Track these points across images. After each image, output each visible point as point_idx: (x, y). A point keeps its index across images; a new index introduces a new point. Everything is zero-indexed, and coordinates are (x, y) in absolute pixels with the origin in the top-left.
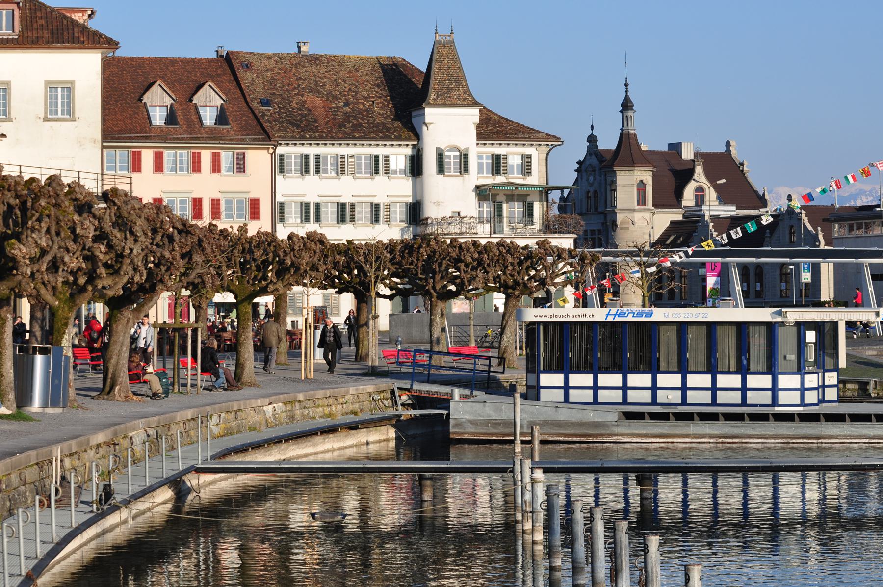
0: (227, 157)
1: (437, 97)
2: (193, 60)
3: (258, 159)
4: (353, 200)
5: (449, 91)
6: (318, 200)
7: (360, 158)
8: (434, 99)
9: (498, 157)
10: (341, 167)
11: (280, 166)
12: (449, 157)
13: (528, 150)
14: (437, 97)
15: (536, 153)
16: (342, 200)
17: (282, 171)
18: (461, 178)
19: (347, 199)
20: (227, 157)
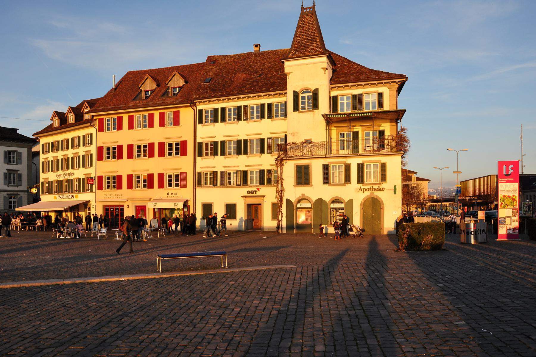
0: (169, 114)
1: (295, 53)
2: (184, 66)
3: (187, 114)
4: (246, 138)
5: (306, 47)
6: (223, 139)
7: (252, 108)
8: (293, 55)
9: (354, 97)
10: (240, 114)
11: (200, 118)
12: (303, 98)
13: (380, 89)
14: (295, 53)
15: (387, 91)
16: (239, 138)
17: (201, 122)
18: (312, 113)
19: (242, 137)
20: (169, 114)
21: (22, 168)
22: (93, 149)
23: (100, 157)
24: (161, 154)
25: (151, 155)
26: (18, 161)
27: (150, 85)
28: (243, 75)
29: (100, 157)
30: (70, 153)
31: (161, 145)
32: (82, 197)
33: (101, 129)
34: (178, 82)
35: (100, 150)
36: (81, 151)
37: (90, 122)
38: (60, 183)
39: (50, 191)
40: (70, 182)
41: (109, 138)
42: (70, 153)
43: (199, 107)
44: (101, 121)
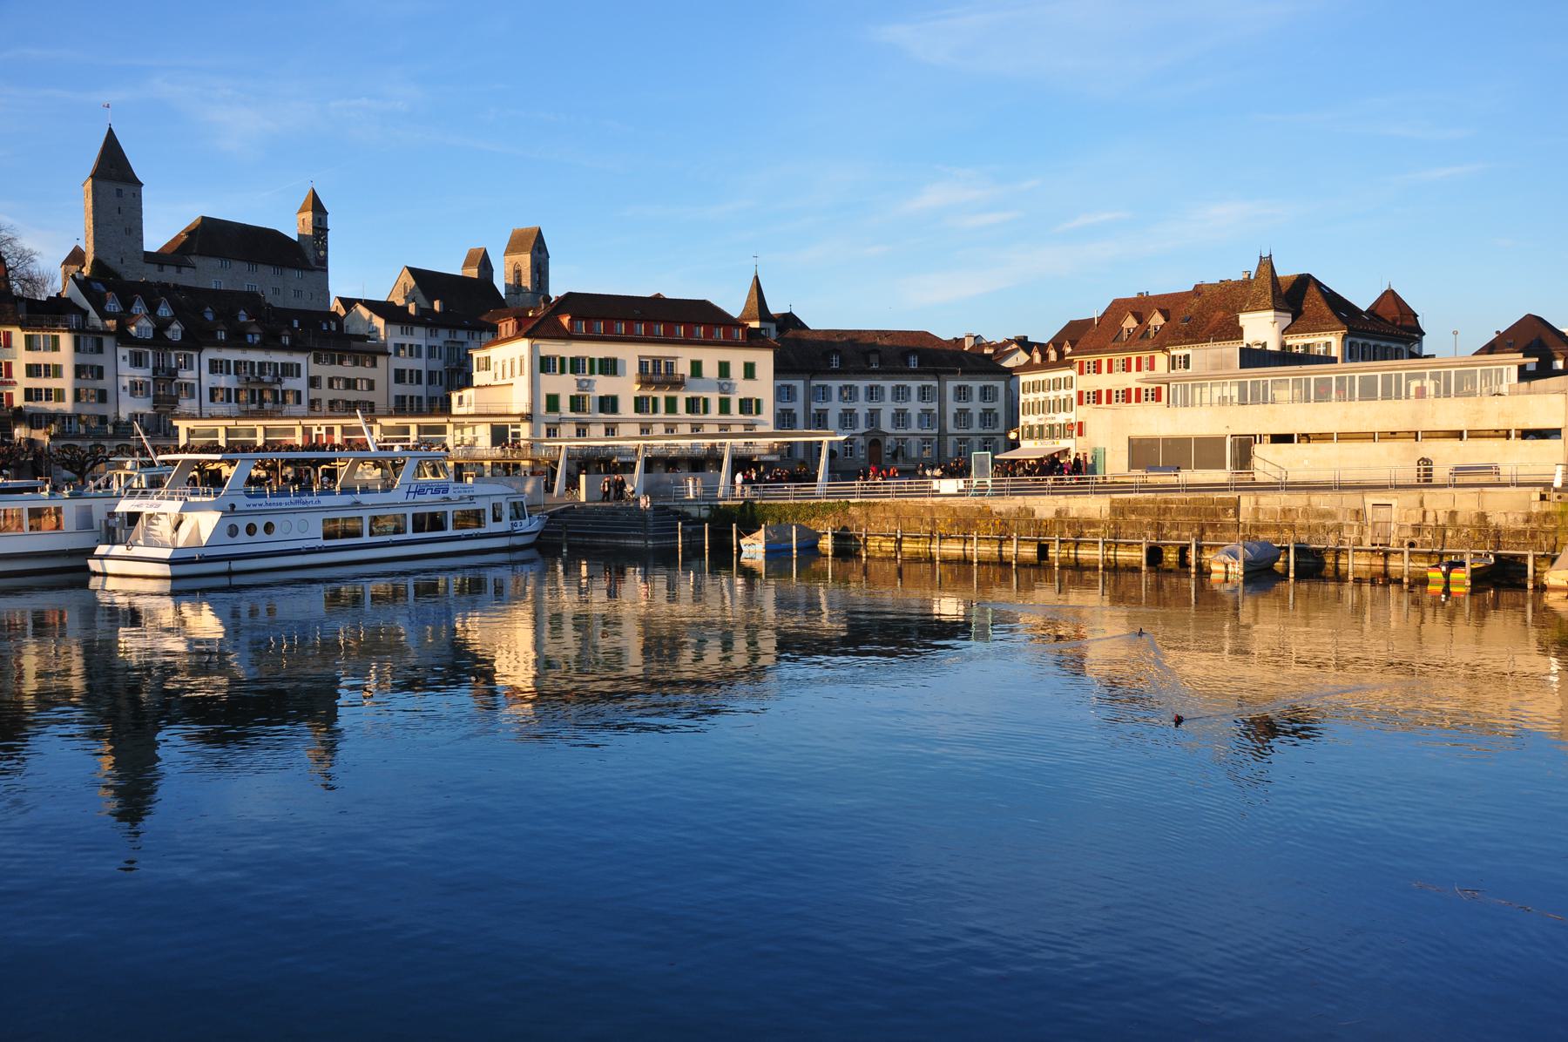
3: (1161, 359)
21: (999, 406)
22: (1073, 393)
23: (1080, 403)
24: (1138, 400)
25: (1129, 401)
26: (995, 399)
27: (1130, 323)
28: (1221, 314)
29: (1080, 403)
30: (1052, 395)
31: (1138, 391)
32: (1063, 444)
33: (1081, 373)
34: (1157, 320)
35: (1080, 394)
36: (1062, 394)
37: (1070, 364)
38: (1041, 427)
39: (1031, 437)
40: (1052, 427)
41: (1090, 382)
42: (1052, 395)
43: (1173, 352)
44: (1081, 363)
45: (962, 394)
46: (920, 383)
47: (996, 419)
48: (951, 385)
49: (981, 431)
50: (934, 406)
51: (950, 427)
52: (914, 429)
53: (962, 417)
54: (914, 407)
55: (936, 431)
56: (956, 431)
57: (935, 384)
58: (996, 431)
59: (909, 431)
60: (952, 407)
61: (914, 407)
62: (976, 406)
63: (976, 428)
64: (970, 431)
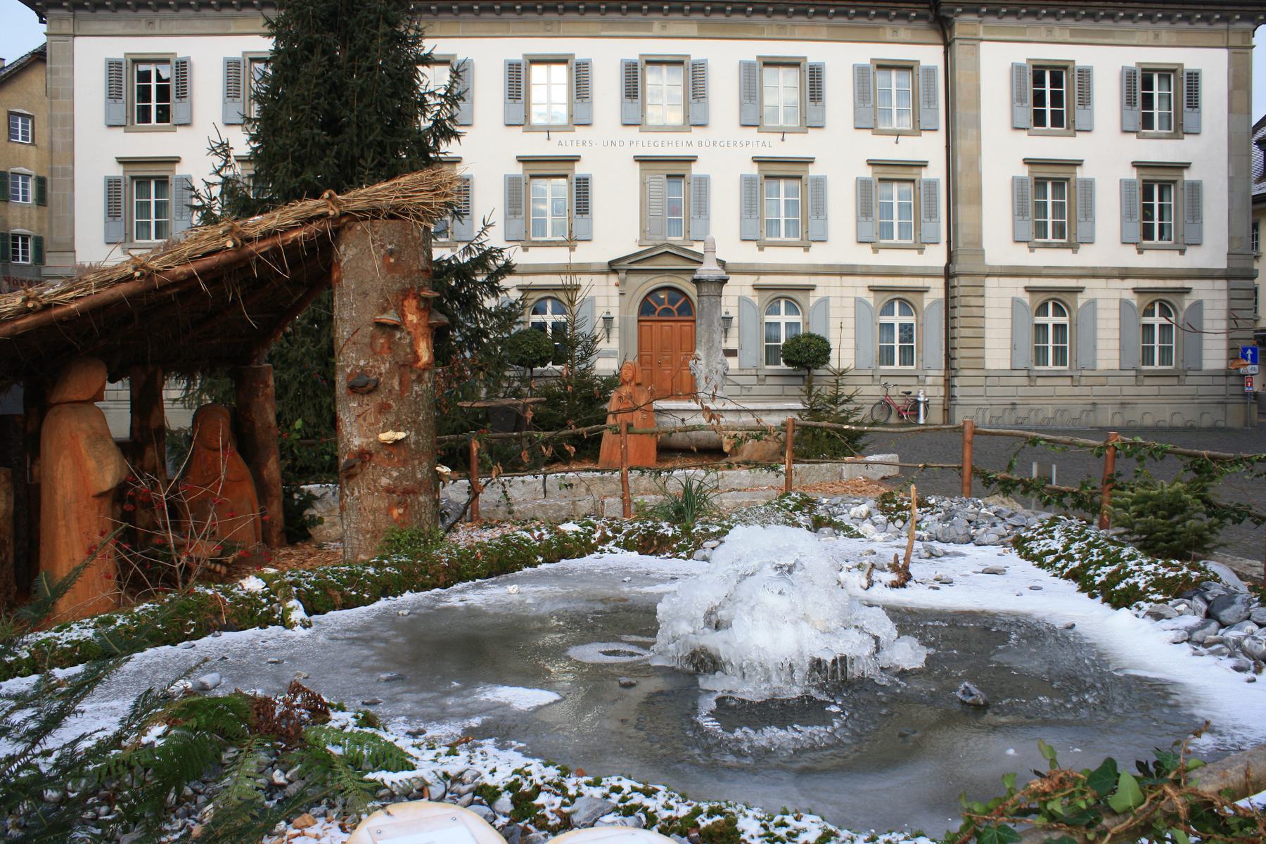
45: (1051, 97)
46: (867, 53)
47: (1195, 213)
48: (999, 59)
49: (1130, 258)
50: (929, 148)
51: (999, 238)
52: (841, 241)
53: (1052, 196)
54: (841, 153)
55: (936, 257)
56: (1022, 257)
57: (930, 55)
58: (1194, 259)
59: (819, 255)
60: (1006, 150)
61: (841, 153)
62: (1106, 151)
63: (1108, 241)
64: (1086, 257)
